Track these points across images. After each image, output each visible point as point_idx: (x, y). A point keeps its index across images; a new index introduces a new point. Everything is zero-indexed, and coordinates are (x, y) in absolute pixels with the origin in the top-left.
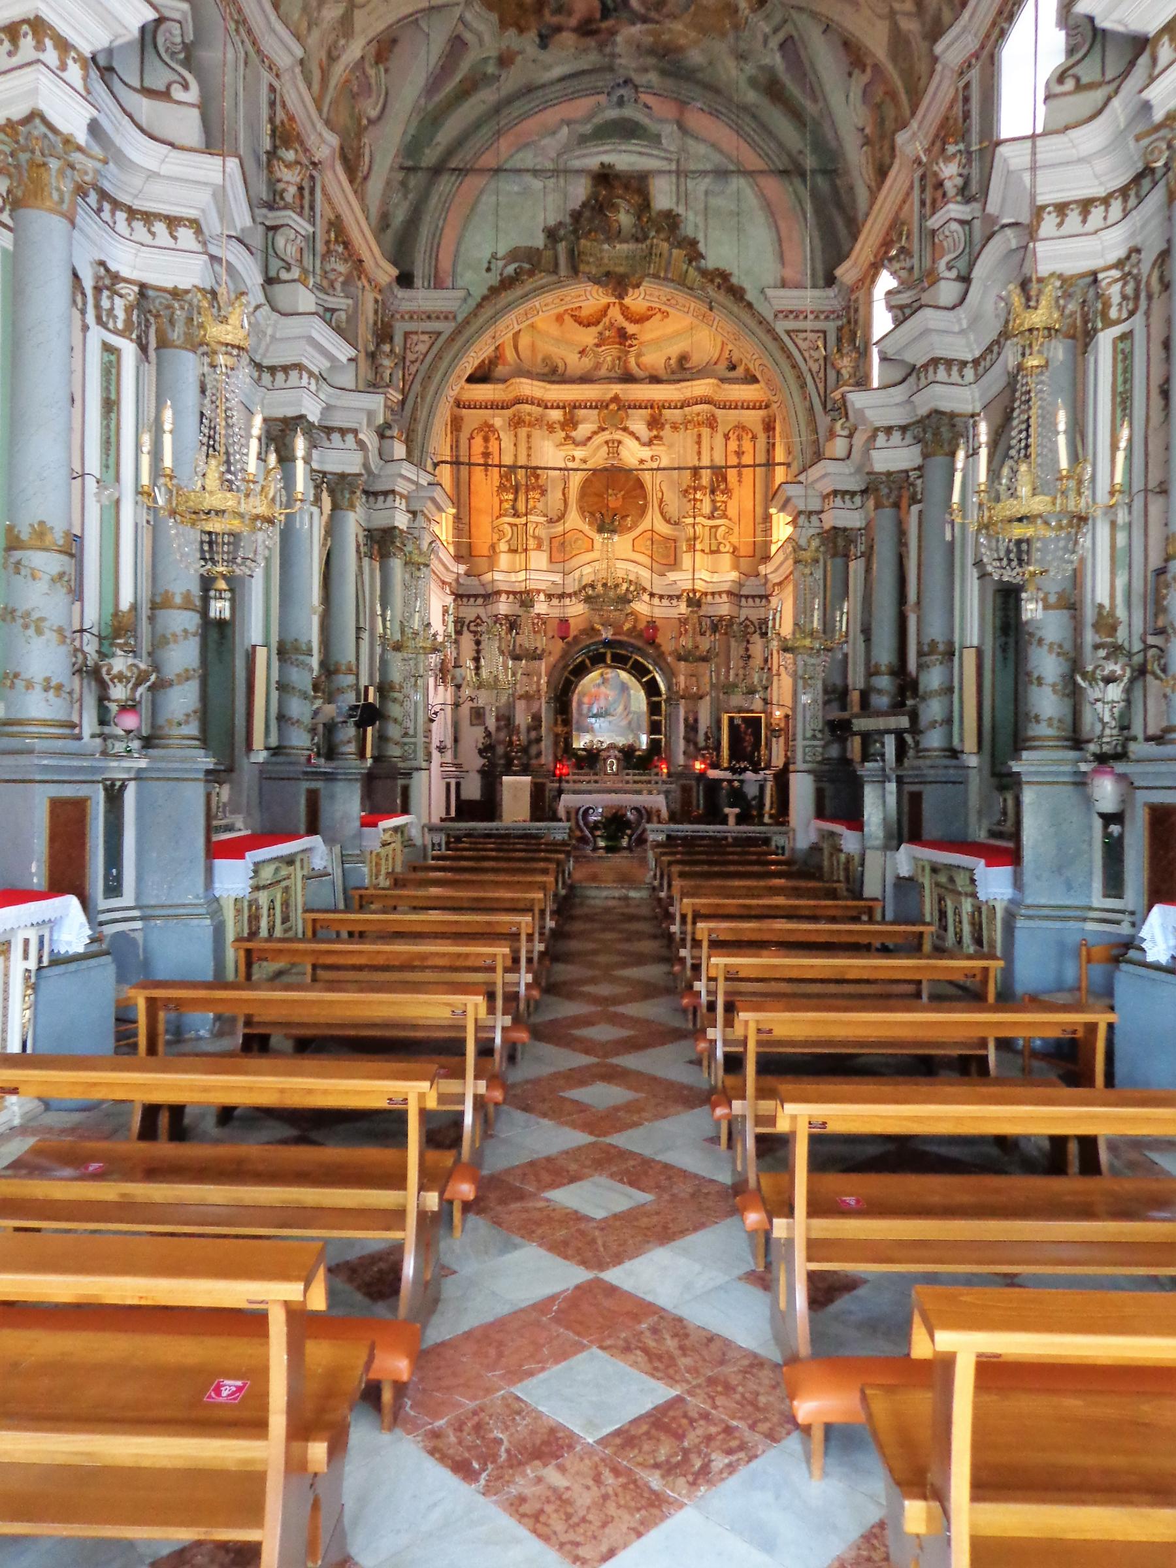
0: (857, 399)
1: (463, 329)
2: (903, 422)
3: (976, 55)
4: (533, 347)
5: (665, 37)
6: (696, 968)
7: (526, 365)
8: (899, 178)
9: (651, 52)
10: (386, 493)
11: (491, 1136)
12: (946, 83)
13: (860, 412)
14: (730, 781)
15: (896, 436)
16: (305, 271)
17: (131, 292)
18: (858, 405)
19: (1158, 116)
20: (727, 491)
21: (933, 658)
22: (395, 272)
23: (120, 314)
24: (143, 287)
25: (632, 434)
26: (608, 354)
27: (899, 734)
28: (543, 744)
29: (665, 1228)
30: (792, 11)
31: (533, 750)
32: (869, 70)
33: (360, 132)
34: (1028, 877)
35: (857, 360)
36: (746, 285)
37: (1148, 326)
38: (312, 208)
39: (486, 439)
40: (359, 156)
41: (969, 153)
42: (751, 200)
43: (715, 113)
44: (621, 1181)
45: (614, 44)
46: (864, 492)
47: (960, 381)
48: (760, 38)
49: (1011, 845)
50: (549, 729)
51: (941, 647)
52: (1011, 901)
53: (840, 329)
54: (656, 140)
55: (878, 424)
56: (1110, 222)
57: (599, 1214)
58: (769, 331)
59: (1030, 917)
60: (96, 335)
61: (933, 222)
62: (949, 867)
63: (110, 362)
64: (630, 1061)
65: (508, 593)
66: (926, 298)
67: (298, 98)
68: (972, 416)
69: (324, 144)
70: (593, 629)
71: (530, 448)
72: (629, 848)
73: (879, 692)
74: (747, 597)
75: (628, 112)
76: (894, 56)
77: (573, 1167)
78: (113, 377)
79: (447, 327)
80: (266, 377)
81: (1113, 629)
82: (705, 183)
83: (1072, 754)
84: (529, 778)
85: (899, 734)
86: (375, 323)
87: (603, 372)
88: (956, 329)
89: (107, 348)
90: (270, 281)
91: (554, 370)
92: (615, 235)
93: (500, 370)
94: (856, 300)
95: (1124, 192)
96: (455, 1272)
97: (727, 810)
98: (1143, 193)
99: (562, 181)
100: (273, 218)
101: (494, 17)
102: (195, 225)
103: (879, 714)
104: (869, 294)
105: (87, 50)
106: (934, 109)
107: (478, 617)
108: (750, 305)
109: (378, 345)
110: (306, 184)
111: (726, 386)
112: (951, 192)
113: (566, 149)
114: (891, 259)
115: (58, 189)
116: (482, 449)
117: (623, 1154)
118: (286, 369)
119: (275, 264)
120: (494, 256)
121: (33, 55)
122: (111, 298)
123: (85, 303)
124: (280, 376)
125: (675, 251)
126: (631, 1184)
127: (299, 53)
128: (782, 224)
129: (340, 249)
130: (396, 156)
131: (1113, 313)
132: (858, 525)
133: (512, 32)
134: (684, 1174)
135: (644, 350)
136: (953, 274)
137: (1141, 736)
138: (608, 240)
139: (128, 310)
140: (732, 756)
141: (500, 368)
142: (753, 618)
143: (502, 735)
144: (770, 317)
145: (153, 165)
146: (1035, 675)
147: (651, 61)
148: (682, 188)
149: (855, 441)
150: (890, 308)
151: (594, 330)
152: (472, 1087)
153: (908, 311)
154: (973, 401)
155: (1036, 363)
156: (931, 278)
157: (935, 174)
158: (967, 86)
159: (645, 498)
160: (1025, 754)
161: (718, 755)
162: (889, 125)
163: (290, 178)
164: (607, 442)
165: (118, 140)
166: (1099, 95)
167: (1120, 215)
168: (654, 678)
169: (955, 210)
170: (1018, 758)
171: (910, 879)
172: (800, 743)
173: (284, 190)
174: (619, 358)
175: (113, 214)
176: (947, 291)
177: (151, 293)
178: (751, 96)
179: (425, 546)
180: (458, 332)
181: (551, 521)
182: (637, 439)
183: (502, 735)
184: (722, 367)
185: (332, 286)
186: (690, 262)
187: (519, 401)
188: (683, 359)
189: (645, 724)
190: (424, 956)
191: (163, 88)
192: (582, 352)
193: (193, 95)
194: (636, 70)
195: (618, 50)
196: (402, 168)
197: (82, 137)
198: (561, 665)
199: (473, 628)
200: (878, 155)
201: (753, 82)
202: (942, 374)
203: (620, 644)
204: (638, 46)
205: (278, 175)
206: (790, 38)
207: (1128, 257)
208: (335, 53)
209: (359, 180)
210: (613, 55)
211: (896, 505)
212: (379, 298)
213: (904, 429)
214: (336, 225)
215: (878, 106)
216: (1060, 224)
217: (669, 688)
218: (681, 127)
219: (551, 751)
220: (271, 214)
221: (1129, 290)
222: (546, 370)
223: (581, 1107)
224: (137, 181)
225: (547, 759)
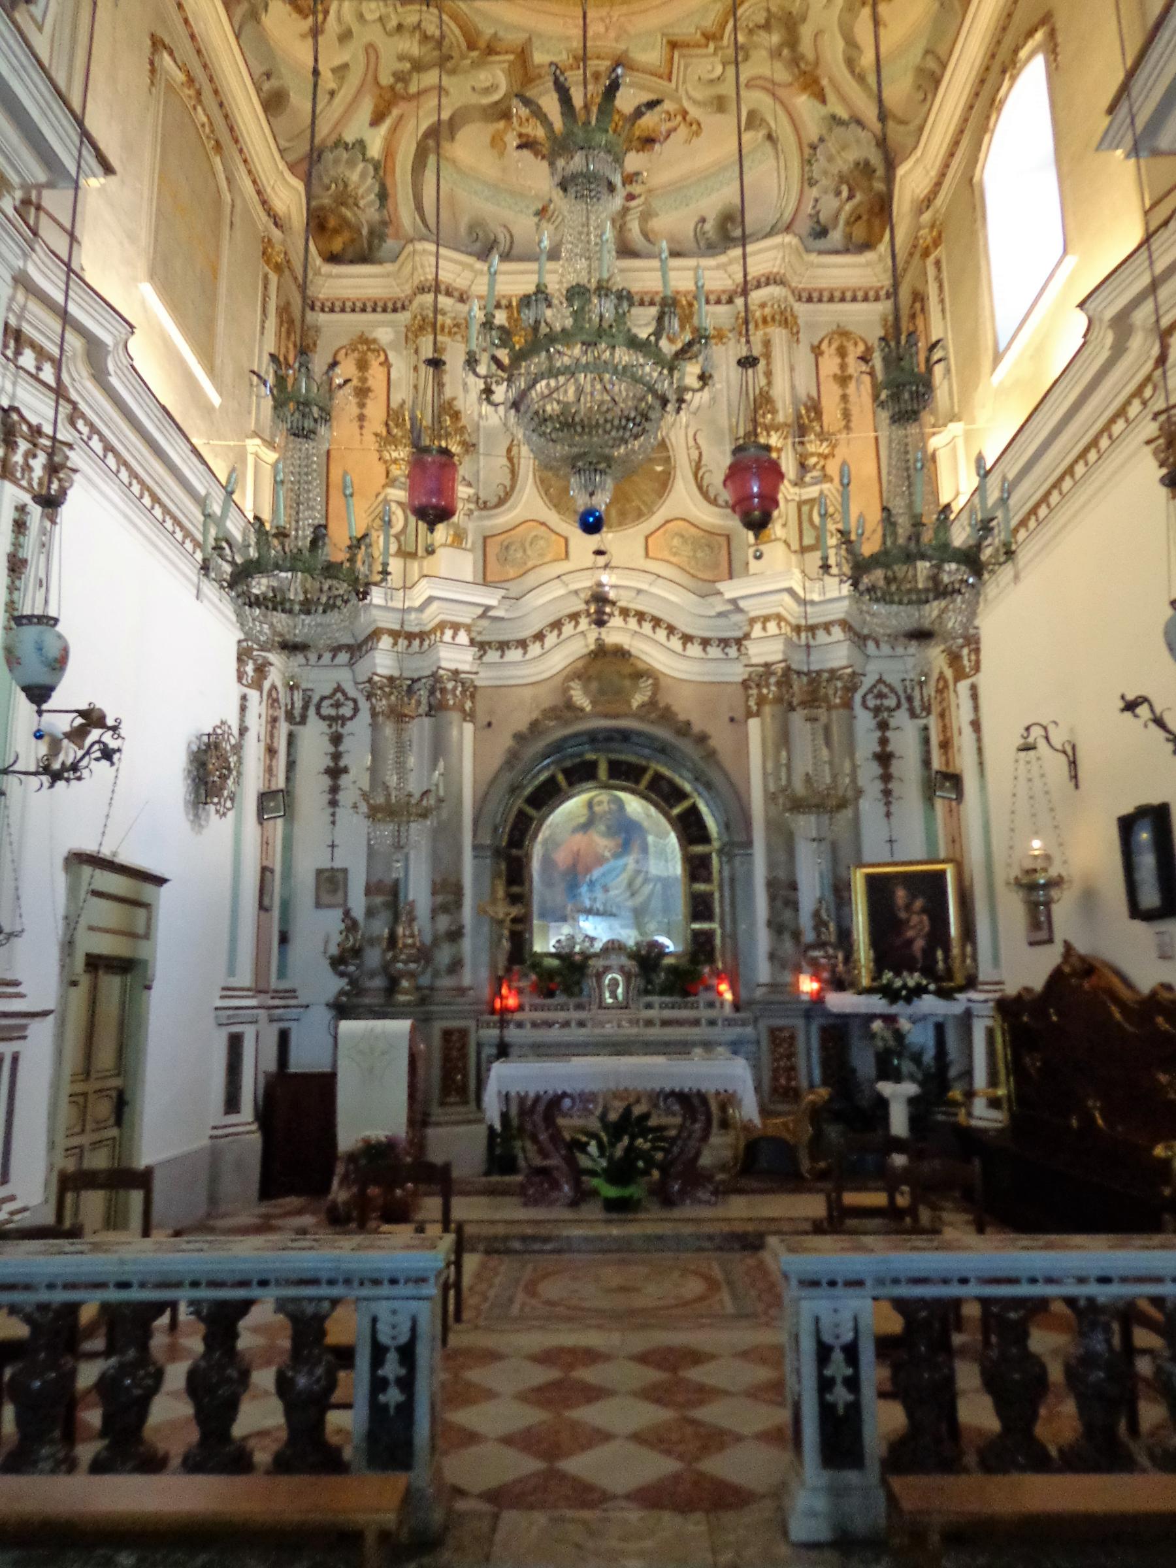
14: (889, 1019)
28: (467, 944)
31: (443, 956)
39: (363, 365)
50: (479, 911)
65: (395, 635)
70: (569, 705)
97: (886, 1088)
107: (339, 689)
135: (656, 204)
140: (882, 961)
142: (893, 679)
159: (667, 460)
161: (849, 958)
168: (694, 811)
181: (485, 506)
184: (804, 225)
189: (680, 906)
198: (507, 778)
199: (327, 711)
203: (625, 736)
217: (727, 826)
219: (485, 958)
225: (476, 973)
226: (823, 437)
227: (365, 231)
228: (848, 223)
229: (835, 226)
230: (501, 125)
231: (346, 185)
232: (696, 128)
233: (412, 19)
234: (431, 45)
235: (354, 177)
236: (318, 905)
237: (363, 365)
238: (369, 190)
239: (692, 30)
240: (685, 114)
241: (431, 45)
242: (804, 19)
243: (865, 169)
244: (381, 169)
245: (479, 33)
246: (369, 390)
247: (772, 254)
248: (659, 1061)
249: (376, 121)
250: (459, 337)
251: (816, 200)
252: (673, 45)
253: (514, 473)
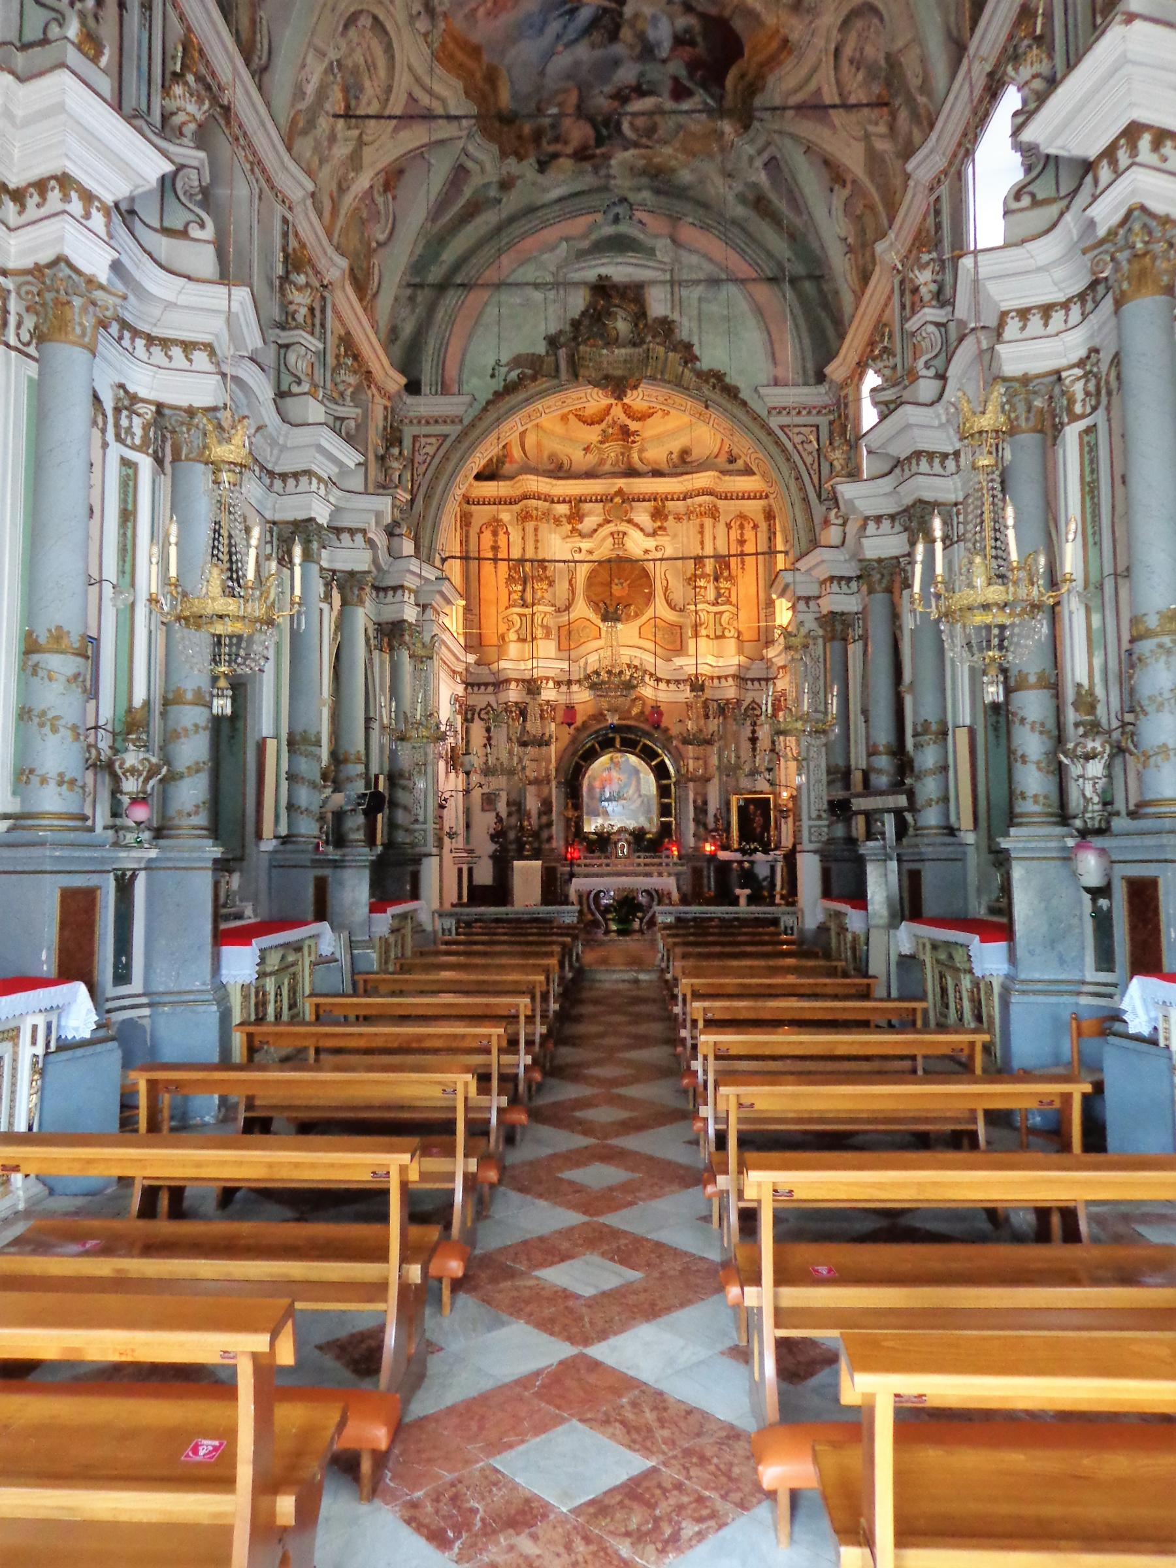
0: (847, 490)
1: (470, 432)
2: (892, 511)
3: (945, 172)
4: (539, 445)
5: (657, 160)
6: (695, 1047)
7: (532, 464)
8: (880, 285)
9: (644, 172)
10: (395, 589)
11: (487, 1217)
12: (919, 196)
13: (850, 502)
14: (740, 862)
15: (886, 524)
16: (315, 386)
17: (149, 411)
18: (847, 496)
19: (1101, 232)
20: (730, 578)
21: (927, 738)
22: (403, 380)
23: (138, 431)
24: (160, 407)
25: (637, 525)
26: (612, 451)
27: (898, 813)
29: (653, 1305)
30: (776, 136)
32: (849, 185)
33: (370, 253)
34: (1020, 952)
35: (847, 452)
36: (741, 384)
37: (1109, 420)
38: (323, 326)
39: (495, 534)
40: (368, 274)
41: (943, 261)
42: (743, 306)
43: (705, 227)
44: (612, 1259)
45: (609, 166)
46: (859, 577)
47: (942, 472)
48: (745, 158)
49: (1004, 920)
50: (560, 814)
51: (934, 727)
52: (1007, 976)
53: (831, 423)
54: (651, 252)
55: (868, 513)
56: (1070, 325)
57: (588, 1292)
58: (763, 426)
59: (1024, 992)
60: (116, 451)
61: (911, 325)
62: (947, 944)
63: (128, 475)
64: (630, 1142)
65: (517, 681)
66: (906, 395)
67: (309, 228)
68: (956, 504)
69: (335, 267)
71: (537, 541)
72: (641, 931)
73: (879, 771)
74: (752, 680)
75: (623, 228)
76: (871, 173)
77: (565, 1245)
78: (131, 490)
79: (453, 430)
80: (278, 484)
81: (1092, 708)
82: (699, 290)
83: (1059, 830)
84: (539, 863)
85: (898, 813)
86: (385, 428)
87: (607, 467)
88: (936, 423)
89: (125, 462)
90: (281, 394)
91: (560, 467)
92: (612, 342)
93: (508, 468)
94: (846, 397)
95: (1081, 297)
96: (441, 1349)
97: (738, 891)
98: (1098, 298)
99: (562, 292)
100: (285, 337)
101: (494, 148)
102: (209, 348)
103: (882, 793)
104: (858, 389)
105: (109, 200)
106: (909, 221)
107: (489, 705)
108: (744, 404)
109: (387, 448)
110: (317, 306)
111: (727, 478)
112: (927, 297)
113: (565, 263)
114: (874, 359)
115: (81, 324)
117: (615, 1233)
118: (296, 475)
119: (286, 380)
120: (498, 363)
121: (60, 206)
122: (129, 418)
123: (105, 423)
124: (291, 482)
125: (671, 354)
126: (623, 1262)
127: (310, 187)
128: (773, 328)
129: (350, 362)
130: (404, 273)
131: (1078, 409)
132: (855, 609)
133: (512, 160)
134: (676, 1253)
136: (932, 372)
137: (1124, 813)
138: (607, 344)
139: (146, 428)
140: (743, 836)
141: (507, 466)
143: (513, 820)
144: (763, 413)
145: (170, 296)
146: (1019, 753)
147: (645, 181)
148: (677, 297)
149: (848, 529)
150: (876, 404)
151: (598, 428)
152: (461, 1165)
153: (892, 406)
154: (956, 490)
155: (986, 462)
156: (912, 376)
157: (912, 280)
158: (938, 199)
160: (1013, 831)
162: (870, 235)
163: (301, 300)
164: (612, 534)
165: (137, 275)
166: (1054, 210)
167: (1079, 318)
168: (663, 762)
169: (931, 313)
170: (1006, 834)
171: (912, 957)
172: (805, 823)
173: (295, 312)
175: (133, 340)
176: (926, 388)
177: (167, 411)
178: (740, 211)
179: (427, 639)
180: (464, 434)
181: (558, 611)
182: (642, 530)
183: (513, 820)
184: (723, 459)
185: (342, 394)
186: (686, 363)
187: (526, 497)
188: (685, 453)
189: (655, 808)
190: (420, 1038)
191: (180, 227)
192: (587, 449)
193: (209, 233)
194: (630, 189)
195: (613, 172)
196: (409, 285)
197: (103, 275)
200: (861, 262)
201: (742, 199)
202: (924, 466)
203: (629, 728)
204: (631, 169)
205: (290, 297)
206: (773, 158)
207: (1088, 357)
208: (344, 186)
209: (368, 297)
210: (608, 176)
211: (889, 590)
212: (389, 404)
213: (892, 517)
214: (347, 341)
215: (859, 218)
216: (1023, 328)
217: (678, 771)
218: (674, 241)
219: (562, 835)
220: (283, 334)
221: (1091, 387)
222: (552, 467)
223: (577, 1188)
224: (156, 311)
225: (558, 843)
226: (730, 578)
236: (483, 810)
237: (495, 534)
248: (641, 879)
253: (573, 591)
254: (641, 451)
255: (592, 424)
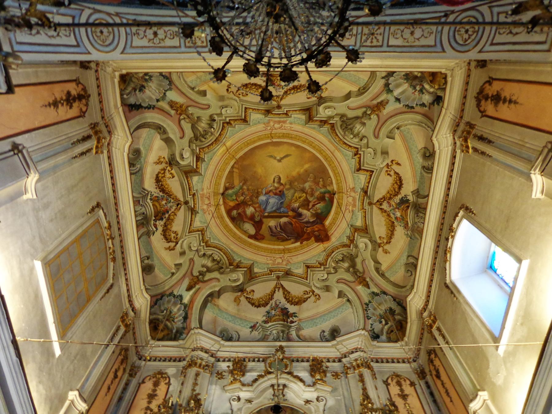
116: (150, 392)
151: (263, 310)
164: (272, 386)
174: (283, 332)
192: (253, 327)
227: (174, 331)
228: (387, 333)
229: (382, 335)
230: (239, 293)
231: (171, 312)
232: (318, 297)
233: (210, 253)
234: (216, 263)
235: (175, 310)
237: (156, 384)
238: (180, 315)
239: (315, 262)
240: (313, 292)
241: (216, 263)
242: (357, 256)
243: (392, 311)
244: (187, 308)
245: (234, 260)
246: (156, 395)
247: (357, 339)
249: (189, 289)
250: (207, 371)
251: (372, 325)
252: (308, 267)
254: (298, 329)
255: (258, 306)
